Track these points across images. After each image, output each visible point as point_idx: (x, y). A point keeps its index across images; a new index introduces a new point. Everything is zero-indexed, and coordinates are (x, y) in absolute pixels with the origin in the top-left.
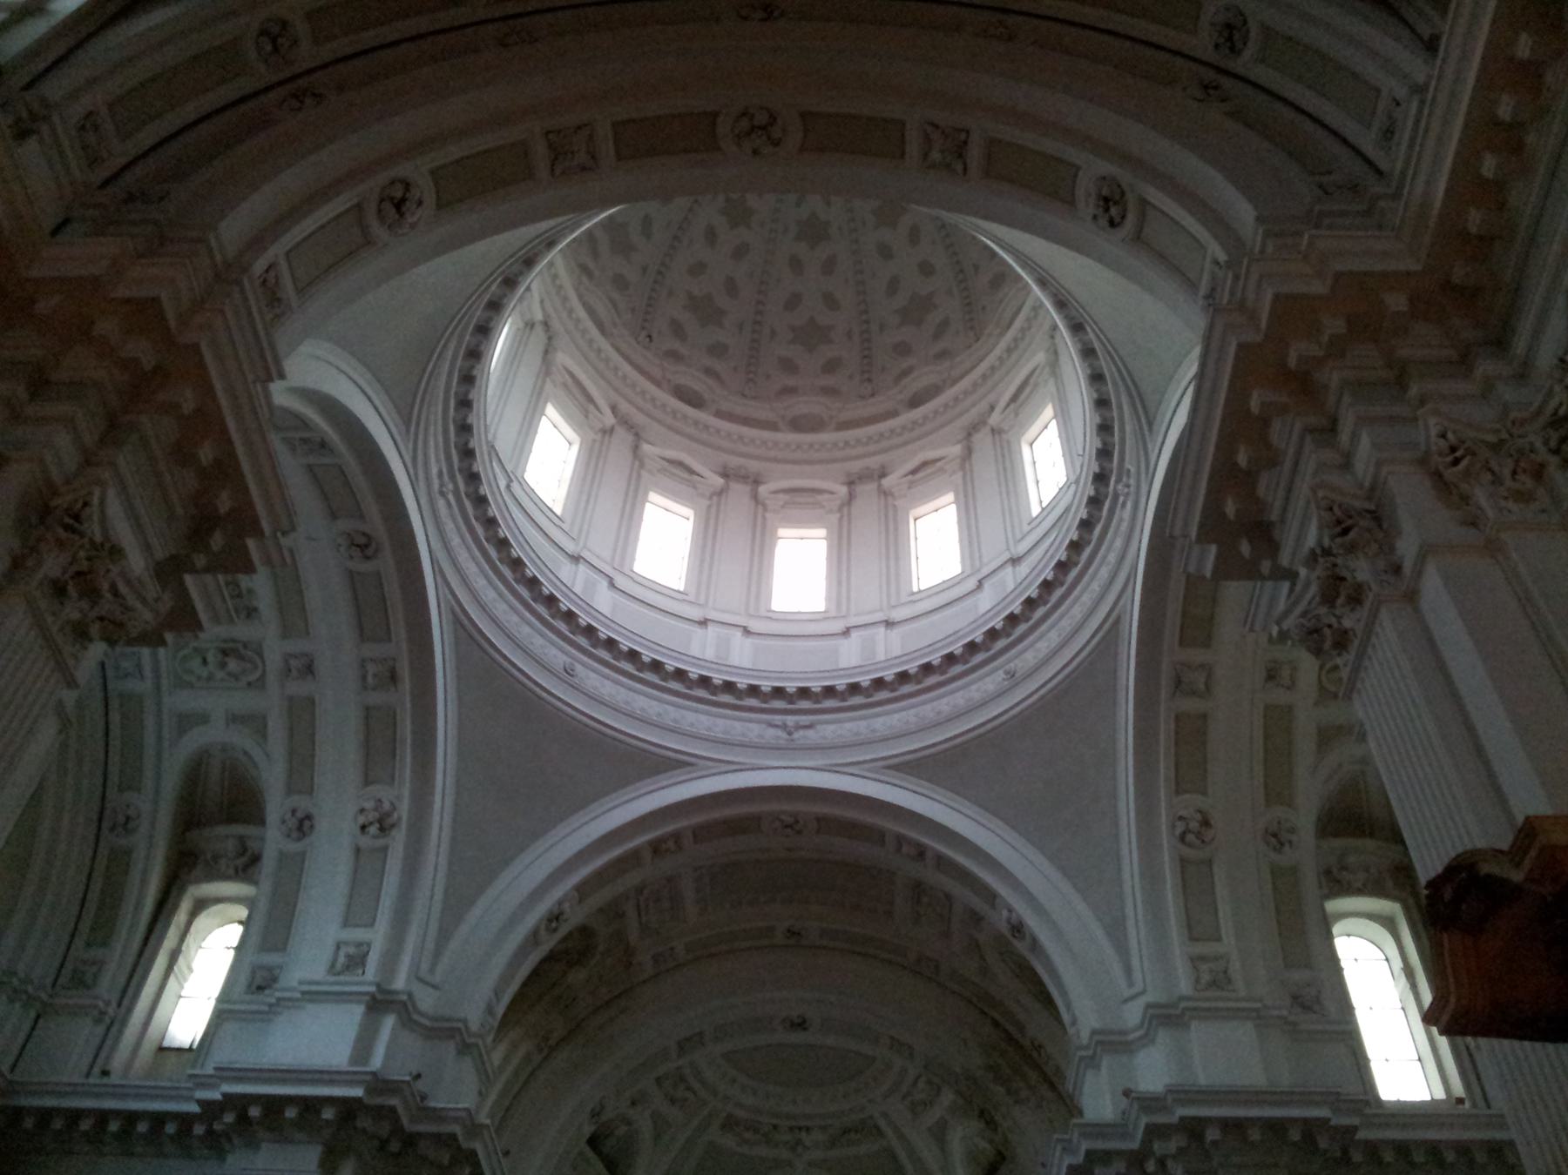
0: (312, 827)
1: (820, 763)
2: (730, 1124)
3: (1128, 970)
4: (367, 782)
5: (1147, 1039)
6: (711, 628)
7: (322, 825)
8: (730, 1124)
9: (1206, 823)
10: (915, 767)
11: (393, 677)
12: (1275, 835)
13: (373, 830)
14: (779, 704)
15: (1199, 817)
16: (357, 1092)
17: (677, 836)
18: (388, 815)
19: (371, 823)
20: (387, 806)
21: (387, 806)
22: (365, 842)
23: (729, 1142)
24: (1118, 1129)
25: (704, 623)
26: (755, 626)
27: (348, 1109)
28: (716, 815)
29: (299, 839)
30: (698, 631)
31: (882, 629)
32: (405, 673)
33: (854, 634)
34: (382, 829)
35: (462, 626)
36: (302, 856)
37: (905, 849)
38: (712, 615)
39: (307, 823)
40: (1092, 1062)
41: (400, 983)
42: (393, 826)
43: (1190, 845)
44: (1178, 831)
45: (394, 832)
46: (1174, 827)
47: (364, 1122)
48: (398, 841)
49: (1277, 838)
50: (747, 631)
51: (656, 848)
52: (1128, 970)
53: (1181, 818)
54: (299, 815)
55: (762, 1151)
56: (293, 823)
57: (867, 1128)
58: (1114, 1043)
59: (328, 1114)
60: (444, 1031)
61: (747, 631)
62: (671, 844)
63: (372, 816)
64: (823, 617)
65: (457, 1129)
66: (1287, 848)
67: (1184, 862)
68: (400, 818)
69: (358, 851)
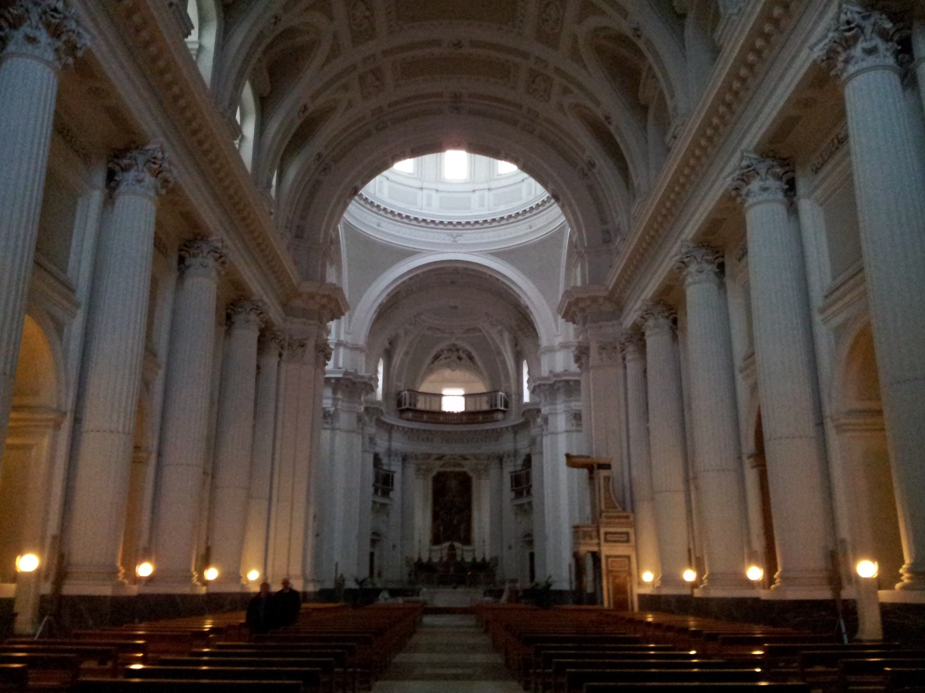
1: (464, 251)
2: (430, 328)
3: (557, 327)
5: (559, 350)
6: (425, 191)
8: (430, 328)
14: (450, 227)
16: (341, 376)
23: (430, 333)
24: (548, 379)
25: (421, 189)
26: (441, 187)
27: (337, 379)
28: (430, 268)
30: (419, 192)
31: (486, 192)
33: (477, 193)
38: (425, 185)
40: (544, 353)
41: (342, 338)
47: (343, 382)
50: (437, 191)
52: (557, 327)
57: (475, 329)
58: (551, 350)
60: (355, 348)
61: (437, 191)
64: (465, 183)
65: (366, 380)
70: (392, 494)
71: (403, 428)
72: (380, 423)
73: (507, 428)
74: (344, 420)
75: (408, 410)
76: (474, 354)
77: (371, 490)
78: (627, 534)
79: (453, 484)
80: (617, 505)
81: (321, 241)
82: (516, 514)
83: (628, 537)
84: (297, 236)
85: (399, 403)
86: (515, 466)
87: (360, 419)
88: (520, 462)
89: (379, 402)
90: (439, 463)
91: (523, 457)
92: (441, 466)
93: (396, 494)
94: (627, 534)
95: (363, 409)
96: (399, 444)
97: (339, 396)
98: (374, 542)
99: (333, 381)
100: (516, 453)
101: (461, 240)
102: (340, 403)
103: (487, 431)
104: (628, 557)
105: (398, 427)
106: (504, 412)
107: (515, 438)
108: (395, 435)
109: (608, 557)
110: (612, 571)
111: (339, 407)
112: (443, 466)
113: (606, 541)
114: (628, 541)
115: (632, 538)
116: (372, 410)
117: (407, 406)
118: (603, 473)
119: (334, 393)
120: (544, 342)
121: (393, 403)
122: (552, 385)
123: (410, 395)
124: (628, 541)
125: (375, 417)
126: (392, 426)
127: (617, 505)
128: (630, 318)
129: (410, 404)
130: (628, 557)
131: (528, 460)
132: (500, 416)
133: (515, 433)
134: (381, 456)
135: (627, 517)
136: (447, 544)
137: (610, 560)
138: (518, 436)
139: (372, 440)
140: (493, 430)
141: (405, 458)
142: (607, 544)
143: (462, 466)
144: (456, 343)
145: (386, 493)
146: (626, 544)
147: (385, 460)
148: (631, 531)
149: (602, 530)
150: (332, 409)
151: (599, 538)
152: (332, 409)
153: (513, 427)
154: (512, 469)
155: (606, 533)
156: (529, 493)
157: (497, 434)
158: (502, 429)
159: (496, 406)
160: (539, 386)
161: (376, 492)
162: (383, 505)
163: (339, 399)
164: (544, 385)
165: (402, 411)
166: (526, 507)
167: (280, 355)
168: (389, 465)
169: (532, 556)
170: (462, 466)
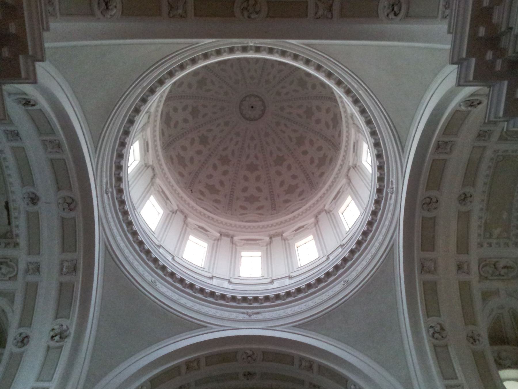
0: (28, 342)
4: (56, 318)
7: (33, 343)
9: (442, 329)
10: (304, 326)
11: (75, 269)
12: (472, 337)
13: (57, 338)
15: (439, 326)
17: (198, 360)
18: (66, 331)
19: (56, 336)
20: (65, 327)
21: (65, 327)
22: (52, 344)
28: (216, 350)
29: (21, 347)
32: (81, 267)
34: (60, 338)
35: (108, 251)
36: (21, 354)
37: (304, 364)
39: (26, 340)
42: (66, 337)
43: (437, 339)
44: (431, 333)
45: (66, 340)
46: (428, 332)
48: (68, 344)
49: (473, 339)
51: (188, 365)
53: (431, 327)
54: (24, 335)
56: (19, 339)
62: (195, 364)
63: (57, 331)
66: (477, 342)
67: (435, 347)
68: (70, 333)
69: (49, 348)
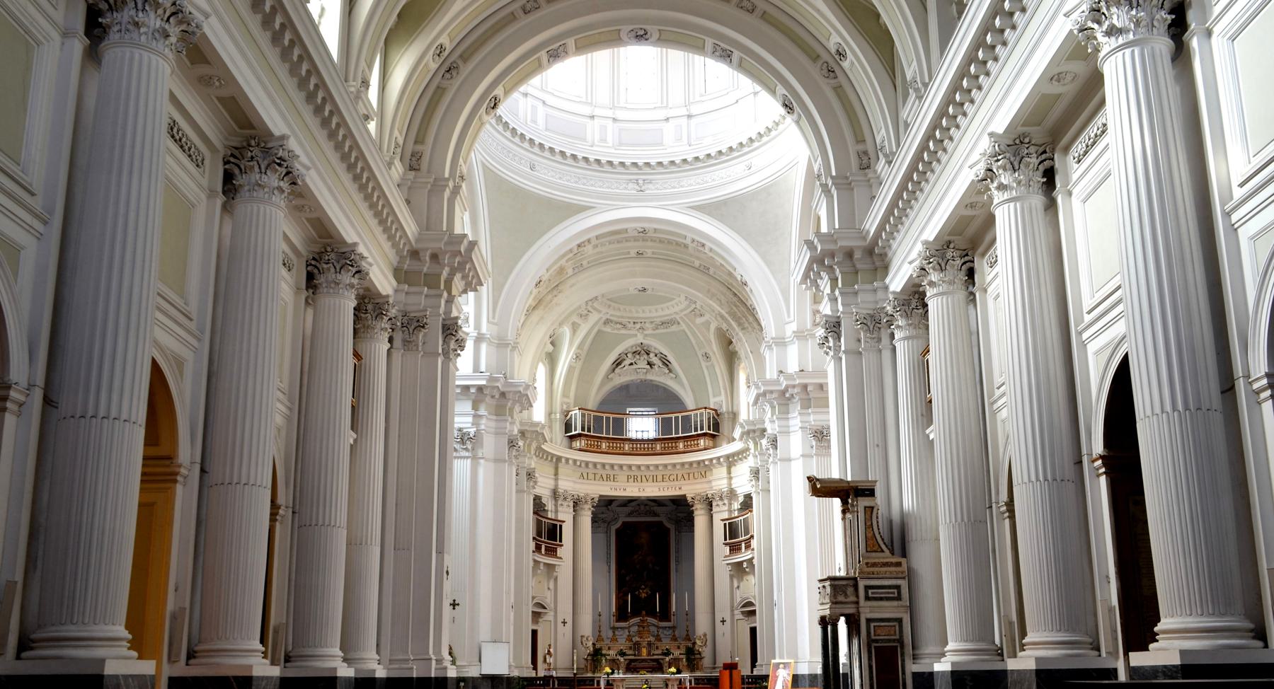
16: (484, 382)
24: (777, 382)
55: (623, 332)
59: (473, 390)
70: (560, 552)
71: (575, 461)
72: (542, 454)
73: (718, 458)
74: (489, 445)
75: (580, 435)
76: (670, 358)
77: (532, 545)
78: (898, 587)
79: (644, 538)
80: (883, 547)
81: (447, 175)
82: (732, 577)
83: (899, 593)
84: (411, 168)
85: (568, 427)
86: (730, 511)
87: (512, 444)
88: (736, 506)
89: (537, 424)
90: (627, 510)
91: (741, 499)
92: (630, 515)
93: (565, 551)
94: (898, 587)
95: (516, 432)
96: (570, 484)
97: (482, 412)
98: (536, 616)
99: (473, 390)
100: (732, 494)
101: (651, 190)
102: (484, 421)
103: (691, 464)
104: (900, 621)
105: (567, 460)
106: (713, 436)
107: (729, 473)
108: (563, 469)
109: (869, 621)
110: (877, 641)
111: (483, 427)
112: (630, 515)
113: (867, 598)
114: (899, 598)
115: (905, 591)
116: (530, 433)
117: (579, 431)
118: (863, 502)
119: (475, 407)
120: (770, 329)
121: (558, 428)
122: (783, 392)
123: (583, 415)
124: (899, 598)
125: (534, 445)
126: (559, 459)
127: (883, 547)
128: (897, 280)
129: (583, 429)
130: (900, 621)
131: (747, 504)
132: (708, 442)
133: (729, 468)
134: (544, 501)
135: (899, 564)
136: (637, 620)
137: (872, 625)
138: (733, 469)
139: (530, 475)
140: (698, 463)
141: (576, 504)
142: (870, 603)
143: (655, 515)
144: (645, 342)
145: (552, 552)
146: (895, 603)
147: (550, 506)
148: (903, 584)
149: (862, 584)
150: (472, 431)
151: (857, 596)
152: (472, 431)
153: (728, 457)
154: (726, 516)
155: (867, 588)
156: (748, 547)
157: (704, 468)
158: (711, 460)
159: (702, 429)
160: (764, 394)
161: (538, 548)
162: (550, 567)
163: (481, 416)
164: (772, 392)
165: (572, 437)
166: (745, 565)
167: (391, 340)
168: (556, 512)
169: (753, 631)
170: (655, 515)
